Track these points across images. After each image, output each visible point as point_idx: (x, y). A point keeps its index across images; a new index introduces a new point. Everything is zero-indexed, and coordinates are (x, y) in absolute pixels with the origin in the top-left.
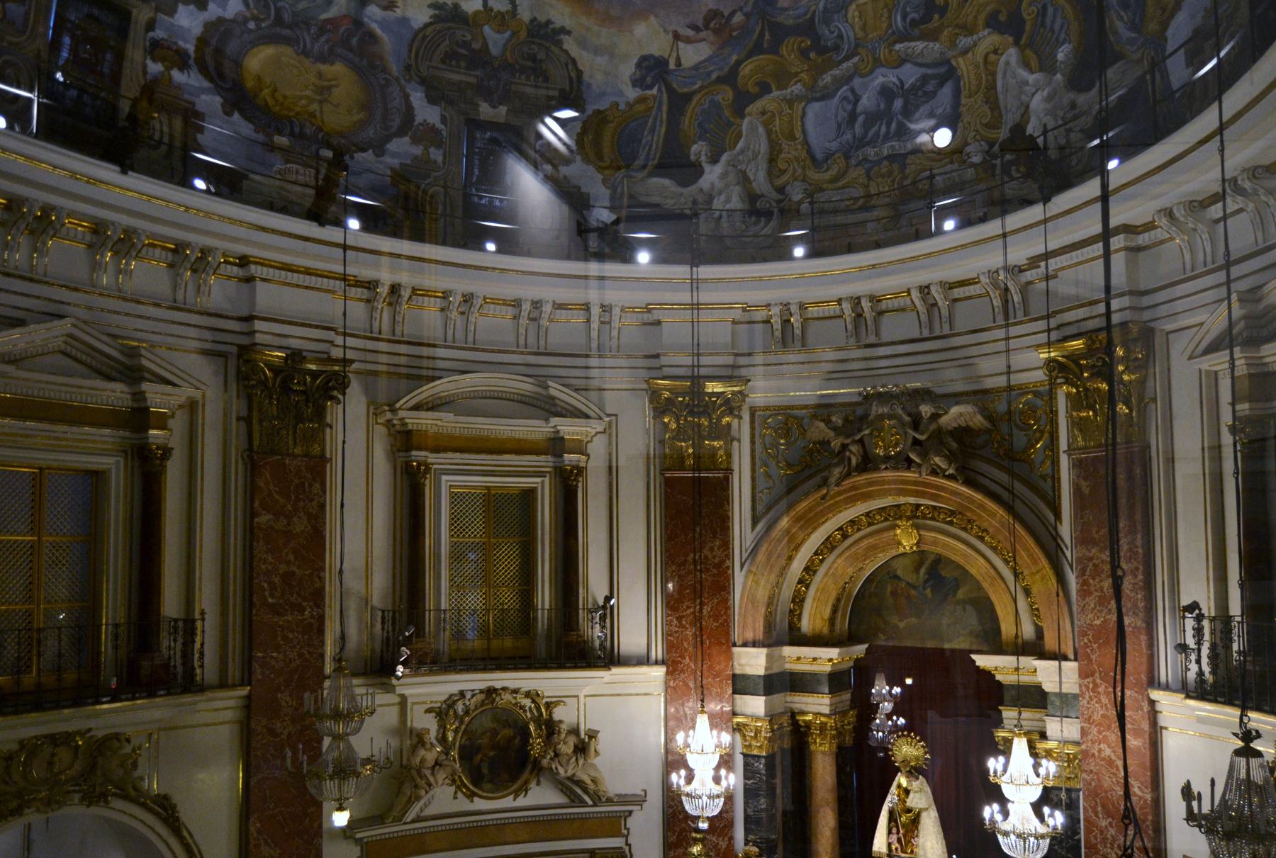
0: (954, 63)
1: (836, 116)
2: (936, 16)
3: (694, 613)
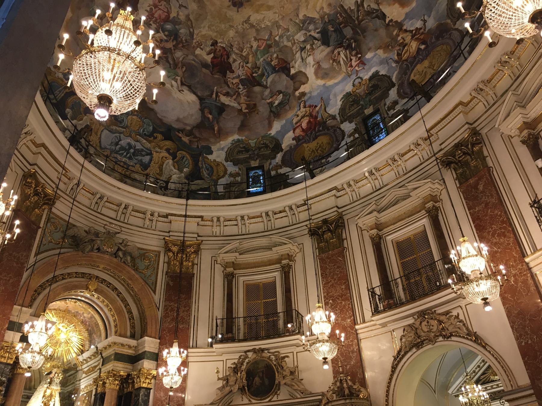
0: (152, 152)
1: (112, 139)
2: (152, 138)
3: (6, 280)
